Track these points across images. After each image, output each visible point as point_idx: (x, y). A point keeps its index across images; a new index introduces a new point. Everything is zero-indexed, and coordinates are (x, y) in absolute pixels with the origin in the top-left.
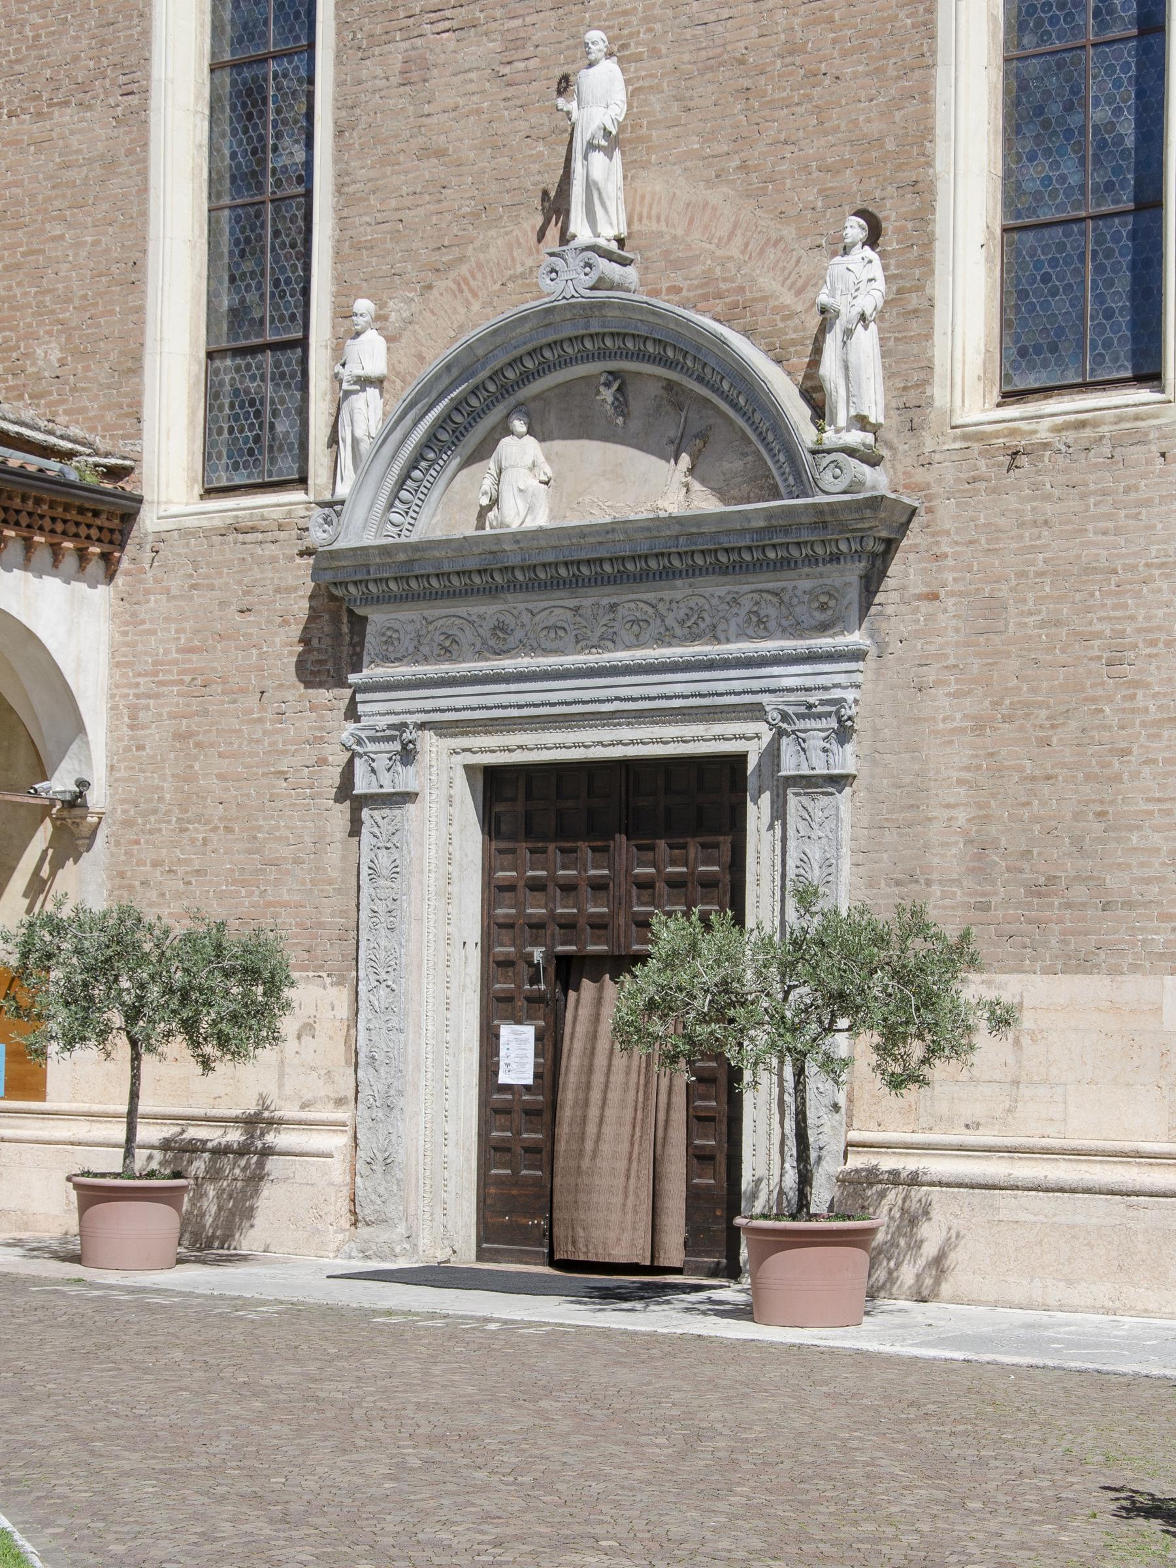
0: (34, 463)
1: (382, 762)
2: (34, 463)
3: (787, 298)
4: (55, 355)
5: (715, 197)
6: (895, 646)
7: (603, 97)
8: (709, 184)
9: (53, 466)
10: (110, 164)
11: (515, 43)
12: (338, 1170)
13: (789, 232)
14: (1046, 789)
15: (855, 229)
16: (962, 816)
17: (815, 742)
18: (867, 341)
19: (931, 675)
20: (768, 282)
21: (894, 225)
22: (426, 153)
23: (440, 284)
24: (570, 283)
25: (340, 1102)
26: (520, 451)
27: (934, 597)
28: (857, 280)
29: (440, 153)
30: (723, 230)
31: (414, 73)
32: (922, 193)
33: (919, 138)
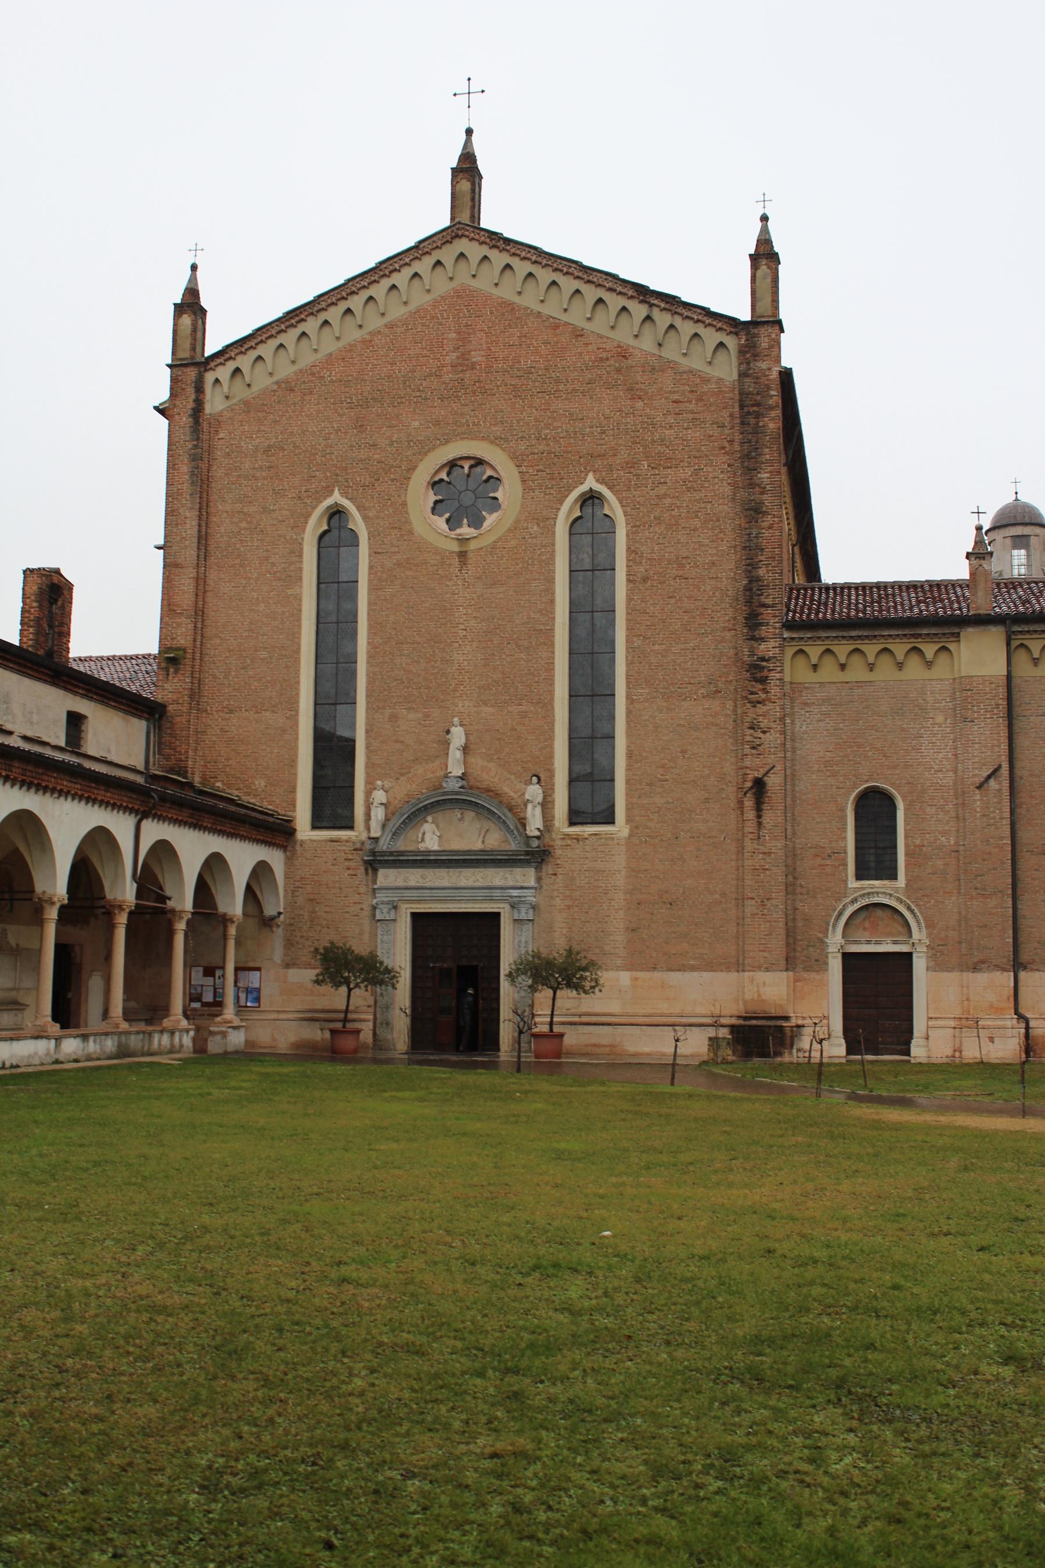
0: (261, 817)
1: (385, 910)
2: (261, 817)
3: (512, 794)
4: (263, 784)
5: (490, 765)
6: (545, 887)
7: (458, 736)
8: (488, 762)
9: (271, 819)
10: (284, 731)
11: (427, 716)
12: (371, 1024)
13: (513, 777)
14: (587, 924)
15: (535, 779)
16: (564, 931)
17: (523, 910)
18: (538, 811)
19: (555, 893)
20: (506, 789)
21: (543, 778)
22: (397, 741)
23: (402, 778)
24: (453, 785)
25: (369, 1006)
26: (428, 827)
27: (555, 874)
28: (534, 792)
29: (402, 742)
30: (492, 774)
31: (394, 718)
32: (551, 773)
33: (551, 756)
